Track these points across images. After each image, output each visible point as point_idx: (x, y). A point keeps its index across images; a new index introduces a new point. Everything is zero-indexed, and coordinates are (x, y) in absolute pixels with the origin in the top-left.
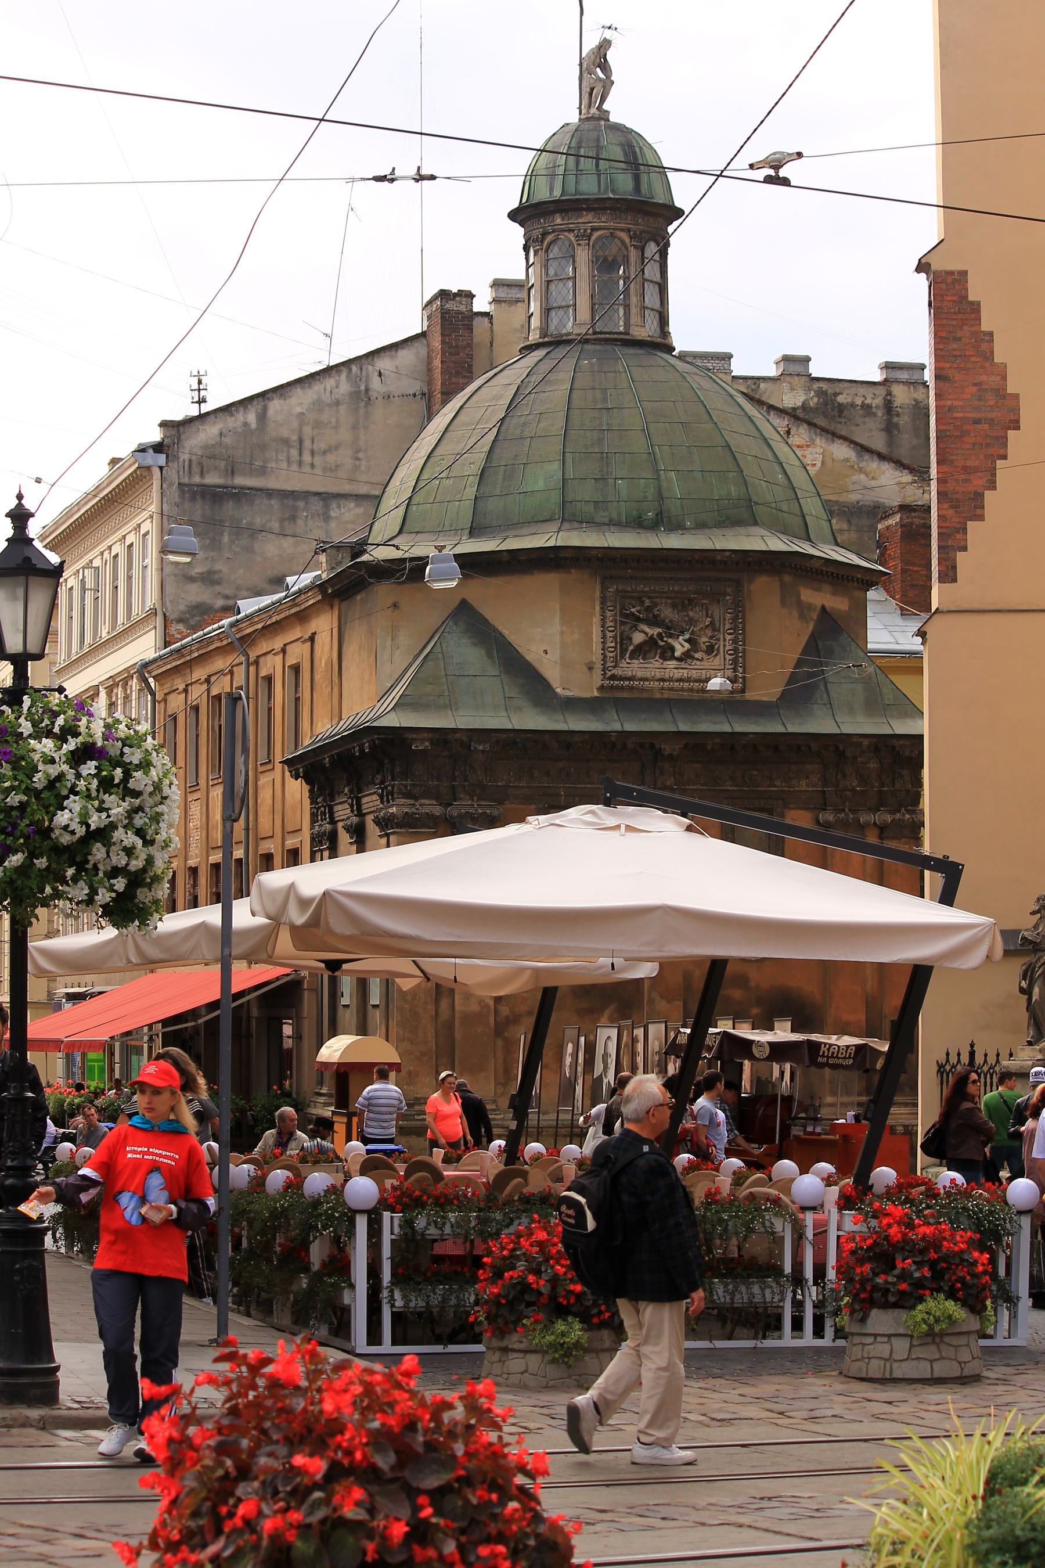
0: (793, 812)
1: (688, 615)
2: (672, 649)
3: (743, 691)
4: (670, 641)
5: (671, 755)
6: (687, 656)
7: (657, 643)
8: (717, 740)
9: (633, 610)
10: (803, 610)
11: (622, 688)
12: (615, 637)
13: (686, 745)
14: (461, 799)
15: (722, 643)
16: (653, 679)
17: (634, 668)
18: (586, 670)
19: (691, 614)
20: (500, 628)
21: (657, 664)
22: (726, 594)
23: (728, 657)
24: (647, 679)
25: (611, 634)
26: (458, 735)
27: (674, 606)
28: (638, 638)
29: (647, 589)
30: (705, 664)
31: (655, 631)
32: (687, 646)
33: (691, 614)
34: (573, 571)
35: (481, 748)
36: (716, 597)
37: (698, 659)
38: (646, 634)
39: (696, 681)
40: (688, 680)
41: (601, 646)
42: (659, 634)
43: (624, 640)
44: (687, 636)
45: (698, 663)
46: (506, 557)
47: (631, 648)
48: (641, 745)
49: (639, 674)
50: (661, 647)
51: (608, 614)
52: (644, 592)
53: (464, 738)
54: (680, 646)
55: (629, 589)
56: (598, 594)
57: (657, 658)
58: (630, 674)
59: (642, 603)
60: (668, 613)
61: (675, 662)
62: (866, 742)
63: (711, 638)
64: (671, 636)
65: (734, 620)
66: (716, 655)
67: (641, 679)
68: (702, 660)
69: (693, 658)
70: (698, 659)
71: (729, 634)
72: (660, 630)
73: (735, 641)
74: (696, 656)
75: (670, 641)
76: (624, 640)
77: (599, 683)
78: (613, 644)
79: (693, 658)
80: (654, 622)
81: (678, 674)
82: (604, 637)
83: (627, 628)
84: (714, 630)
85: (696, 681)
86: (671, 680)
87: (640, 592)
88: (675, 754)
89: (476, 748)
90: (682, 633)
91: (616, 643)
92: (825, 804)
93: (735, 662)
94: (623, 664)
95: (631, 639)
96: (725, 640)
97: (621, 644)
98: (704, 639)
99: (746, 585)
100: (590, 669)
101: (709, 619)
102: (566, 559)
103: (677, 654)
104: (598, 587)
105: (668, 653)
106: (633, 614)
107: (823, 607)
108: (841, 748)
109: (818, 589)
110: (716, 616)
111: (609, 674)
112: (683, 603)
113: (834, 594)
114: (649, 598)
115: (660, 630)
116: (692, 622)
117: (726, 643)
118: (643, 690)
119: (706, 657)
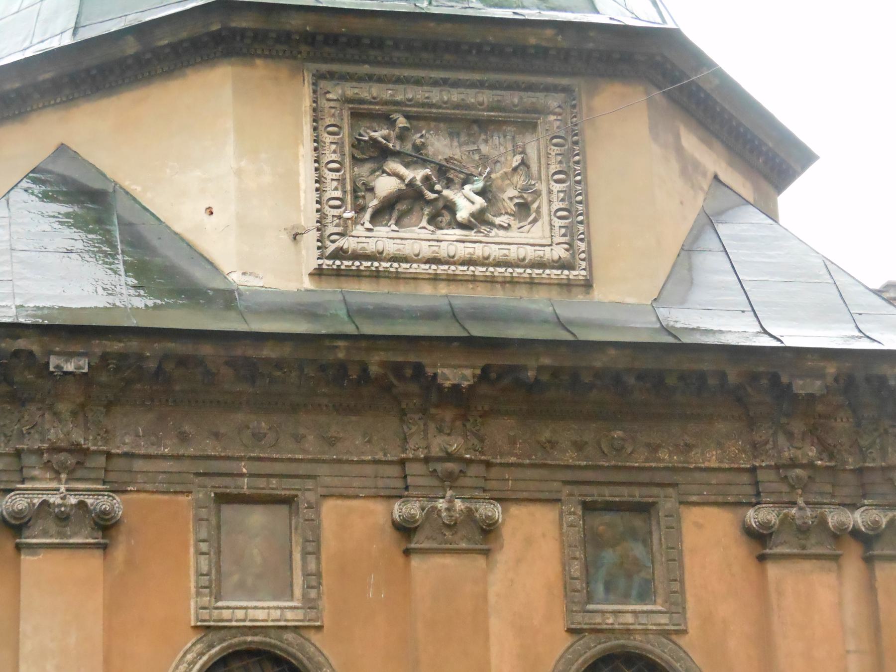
0: (696, 510)
1: (478, 151)
2: (451, 208)
3: (588, 285)
4: (446, 192)
5: (456, 388)
6: (479, 220)
8: (546, 361)
9: (373, 134)
10: (689, 169)
11: (358, 275)
12: (342, 181)
13: (485, 370)
14: (33, 479)
17: (384, 238)
18: (286, 238)
19: (485, 149)
20: (127, 184)
21: (424, 234)
22: (545, 111)
23: (557, 223)
24: (404, 259)
25: (334, 175)
26: (21, 344)
27: (453, 135)
28: (386, 185)
29: (399, 98)
30: (514, 235)
31: (417, 174)
32: (480, 202)
33: (485, 149)
34: (259, 62)
35: (70, 367)
36: (527, 123)
37: (501, 227)
38: (401, 178)
39: (498, 264)
40: (484, 262)
41: (315, 196)
42: (427, 179)
43: (360, 191)
44: (479, 185)
45: (502, 233)
46: (131, 47)
47: (375, 202)
48: (397, 369)
49: (391, 248)
50: (429, 202)
51: (328, 139)
52: (396, 103)
53: (35, 348)
54: (466, 202)
55: (365, 95)
56: (307, 103)
57: (424, 223)
58: (371, 247)
59: (392, 123)
60: (440, 146)
61: (458, 233)
62: (831, 369)
63: (524, 189)
64: (449, 184)
65: (567, 156)
66: (535, 221)
67: (394, 259)
68: (507, 228)
69: (492, 225)
70: (501, 227)
71: (558, 181)
72: (428, 171)
73: (568, 195)
74: (497, 221)
75: (446, 192)
76: (360, 191)
77: (314, 264)
78: (338, 194)
79: (492, 225)
80: (417, 158)
81: (462, 251)
83: (364, 170)
84: (529, 176)
85: (498, 264)
86: (450, 261)
87: (386, 103)
88: (465, 384)
89: (58, 367)
91: (344, 192)
92: (758, 494)
93: (570, 230)
94: (359, 230)
95: (371, 190)
96: (550, 192)
97: (356, 197)
98: (511, 192)
100: (295, 237)
101: (517, 159)
102: (242, 32)
103: (462, 215)
104: (307, 91)
105: (442, 214)
106: (374, 141)
107: (716, 178)
108: (785, 379)
109: (709, 145)
110: (532, 153)
111: (331, 247)
112: (469, 124)
113: (731, 164)
114: (408, 117)
115: (428, 171)
116: (485, 160)
117: (551, 198)
118: (397, 277)
119: (515, 224)
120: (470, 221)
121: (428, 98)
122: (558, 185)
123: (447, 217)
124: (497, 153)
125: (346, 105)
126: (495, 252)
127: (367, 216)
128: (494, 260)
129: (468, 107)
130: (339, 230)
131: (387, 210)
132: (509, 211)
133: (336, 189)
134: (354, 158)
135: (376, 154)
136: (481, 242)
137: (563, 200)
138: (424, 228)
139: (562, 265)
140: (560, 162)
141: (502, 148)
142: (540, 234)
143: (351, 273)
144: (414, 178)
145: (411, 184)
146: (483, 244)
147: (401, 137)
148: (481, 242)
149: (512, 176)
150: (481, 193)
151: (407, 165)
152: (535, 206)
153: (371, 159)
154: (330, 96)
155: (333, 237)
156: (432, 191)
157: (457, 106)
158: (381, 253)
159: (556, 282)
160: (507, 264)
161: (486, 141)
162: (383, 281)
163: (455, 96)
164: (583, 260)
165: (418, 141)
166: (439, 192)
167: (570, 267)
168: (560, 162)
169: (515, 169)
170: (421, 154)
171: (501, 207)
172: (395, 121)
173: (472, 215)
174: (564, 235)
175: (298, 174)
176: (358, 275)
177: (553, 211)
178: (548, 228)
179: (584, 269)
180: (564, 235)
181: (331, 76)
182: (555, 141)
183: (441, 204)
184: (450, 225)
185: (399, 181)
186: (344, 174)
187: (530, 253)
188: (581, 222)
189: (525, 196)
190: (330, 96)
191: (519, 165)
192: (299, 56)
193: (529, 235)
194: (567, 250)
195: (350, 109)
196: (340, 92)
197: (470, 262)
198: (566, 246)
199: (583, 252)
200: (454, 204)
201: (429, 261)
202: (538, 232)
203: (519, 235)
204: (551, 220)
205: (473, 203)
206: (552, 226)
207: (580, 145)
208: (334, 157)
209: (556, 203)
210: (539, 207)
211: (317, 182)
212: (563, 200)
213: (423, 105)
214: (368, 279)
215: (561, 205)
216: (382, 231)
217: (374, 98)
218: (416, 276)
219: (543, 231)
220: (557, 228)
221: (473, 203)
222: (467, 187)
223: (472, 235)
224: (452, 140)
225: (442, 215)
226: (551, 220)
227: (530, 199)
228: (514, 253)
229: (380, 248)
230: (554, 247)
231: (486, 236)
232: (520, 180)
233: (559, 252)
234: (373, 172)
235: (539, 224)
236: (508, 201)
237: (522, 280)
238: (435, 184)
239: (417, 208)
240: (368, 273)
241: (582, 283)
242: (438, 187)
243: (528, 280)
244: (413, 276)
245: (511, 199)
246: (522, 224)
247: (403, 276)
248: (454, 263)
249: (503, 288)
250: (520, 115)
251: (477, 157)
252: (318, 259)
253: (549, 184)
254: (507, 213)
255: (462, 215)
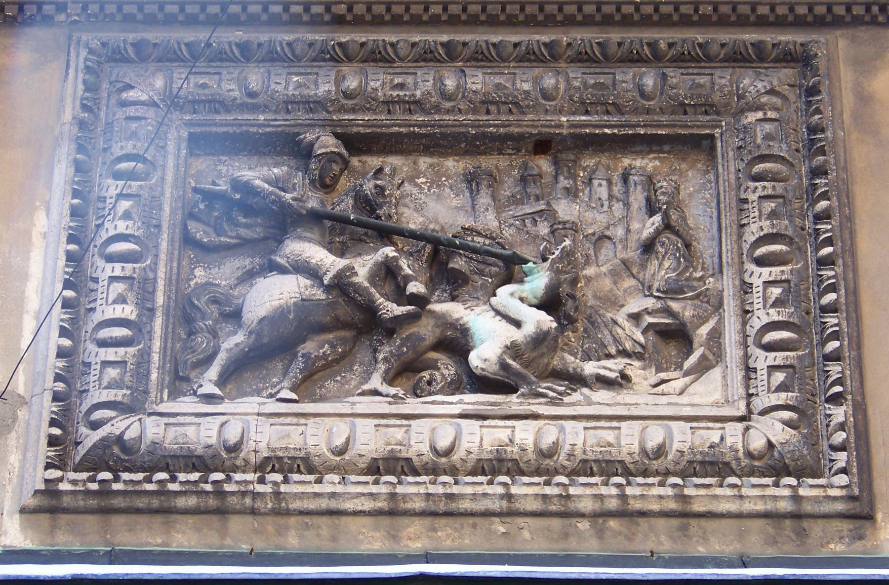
1: (549, 214)
2: (457, 343)
3: (860, 513)
7: (370, 310)
15: (730, 306)
16: (341, 462)
19: (565, 210)
23: (762, 360)
24: (306, 464)
31: (362, 267)
32: (538, 320)
33: (565, 210)
38: (312, 272)
42: (388, 273)
44: (538, 281)
45: (602, 395)
47: (234, 341)
51: (113, 188)
52: (312, 104)
57: (376, 382)
58: (204, 434)
60: (434, 201)
63: (673, 291)
64: (454, 284)
66: (702, 368)
67: (272, 463)
69: (577, 380)
72: (389, 251)
74: (590, 368)
78: (128, 311)
81: (478, 439)
82: (77, 280)
85: (584, 468)
86: (442, 463)
90: (510, 269)
91: (147, 310)
95: (235, 316)
96: (746, 288)
98: (635, 305)
99: (846, 75)
103: (485, 355)
110: (698, 215)
111: (91, 438)
120: (504, 366)
121: (401, 86)
122: (766, 271)
123: (447, 368)
124: (602, 219)
125: (176, 115)
126: (577, 438)
127: (213, 372)
128: (571, 455)
129: (516, 105)
130: (118, 395)
131: (273, 351)
132: (628, 345)
133: (121, 300)
134: (188, 241)
135: (257, 233)
136: (535, 417)
137: (778, 303)
138: (376, 393)
139: (773, 465)
140: (773, 215)
141: (618, 207)
142: (718, 396)
143: (141, 503)
144: (350, 268)
145: (341, 285)
146: (541, 423)
147: (325, 185)
148: (535, 417)
149: (643, 266)
150: (549, 303)
151: (341, 253)
152: (704, 331)
153: (243, 245)
154: (132, 95)
155: (98, 415)
156: (401, 297)
157: (486, 103)
158: (234, 449)
159: (760, 507)
160: (607, 467)
161: (572, 193)
162: (236, 523)
163: (478, 81)
164: (842, 448)
165: (369, 187)
166: (420, 301)
167: (804, 471)
168: (773, 215)
169: (648, 247)
170: (378, 217)
171: (608, 339)
172: (311, 145)
173: (513, 349)
174: (783, 387)
175: (24, 277)
176: (164, 509)
177: (752, 332)
178: (739, 375)
179: (844, 471)
180: (783, 387)
181: (142, 54)
182: (759, 168)
183: (426, 330)
184: (454, 387)
185: (304, 282)
186: (154, 268)
187: (682, 439)
188: (835, 357)
189: (675, 306)
190: (132, 95)
191: (658, 233)
192: (62, 17)
193: (684, 399)
194: (788, 423)
195: (190, 124)
196: (159, 83)
197: (496, 465)
198: (786, 415)
199: (842, 427)
200: (464, 330)
201: (375, 468)
202: (710, 392)
203: (651, 399)
204: (746, 357)
205: (517, 324)
206: (749, 371)
207: (832, 176)
208: (122, 227)
209: (761, 313)
210: (716, 335)
211: (67, 285)
212: (778, 303)
213: (389, 103)
214: (191, 520)
215: (775, 315)
216: (250, 404)
217: (252, 95)
218: (333, 504)
219: (725, 386)
220: (762, 374)
221: (517, 324)
222: (504, 291)
223: (513, 403)
224: (474, 194)
225: (433, 366)
226: (746, 357)
227: (688, 313)
228: (628, 440)
229: (232, 435)
230: (758, 422)
231: (553, 402)
232: (661, 270)
233: (773, 430)
234: (249, 276)
235: (716, 373)
236: (627, 325)
237: (655, 507)
238: (407, 279)
239: (363, 354)
240: (192, 501)
241: (840, 507)
242: (415, 288)
243: (672, 505)
244: (324, 504)
245: (635, 317)
246: (663, 375)
247: (296, 505)
248: (453, 471)
249: (600, 533)
250: (664, 118)
251: (543, 229)
252: (48, 466)
253: (741, 272)
254: (624, 353)
255: (485, 355)
